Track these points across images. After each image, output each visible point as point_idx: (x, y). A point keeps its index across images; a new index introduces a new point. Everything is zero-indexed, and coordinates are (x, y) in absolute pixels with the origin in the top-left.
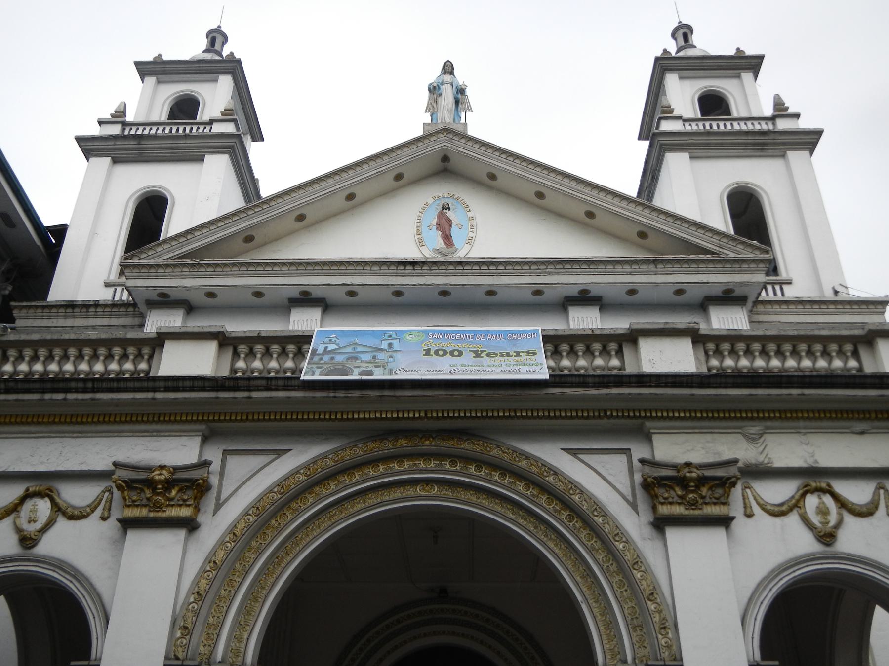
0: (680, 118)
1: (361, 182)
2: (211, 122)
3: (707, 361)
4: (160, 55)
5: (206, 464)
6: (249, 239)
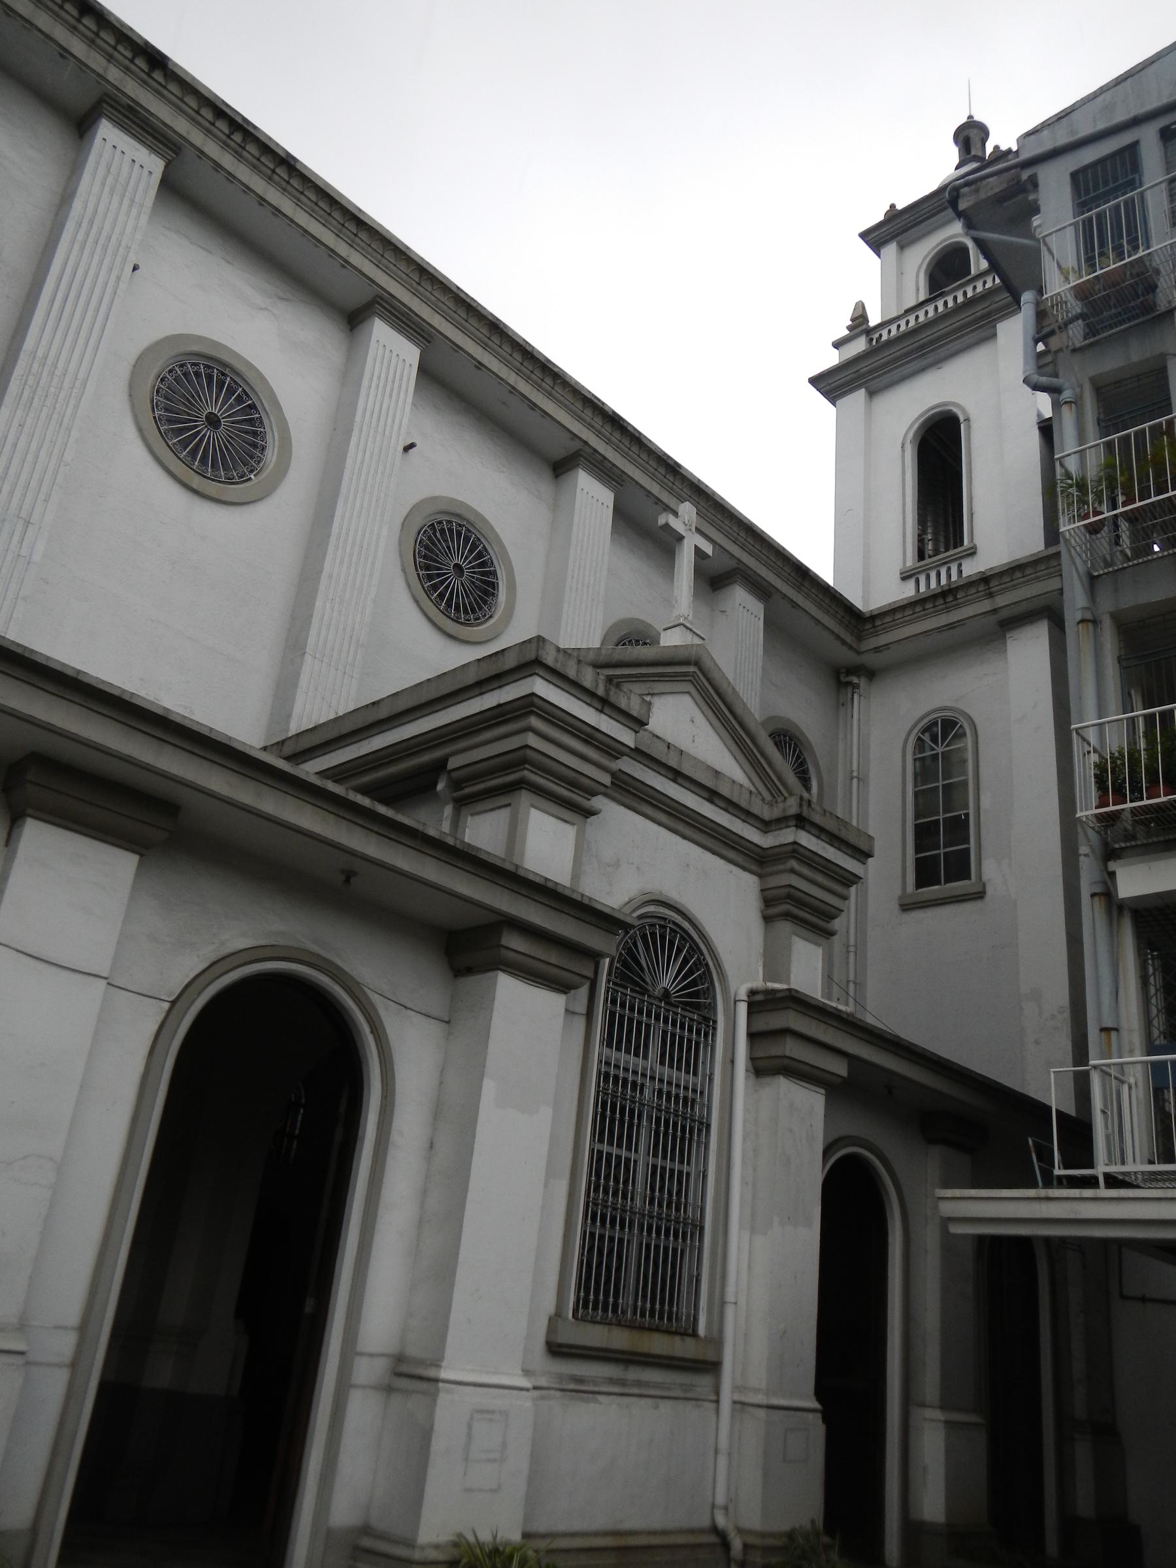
4: (893, 206)
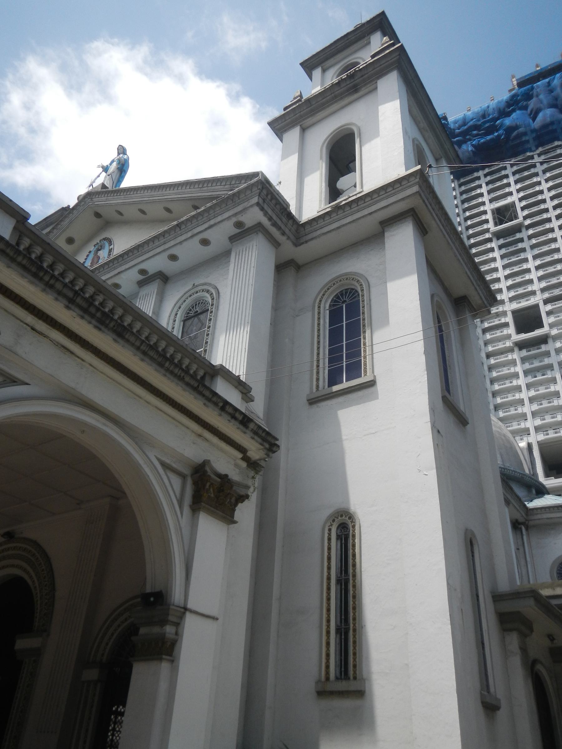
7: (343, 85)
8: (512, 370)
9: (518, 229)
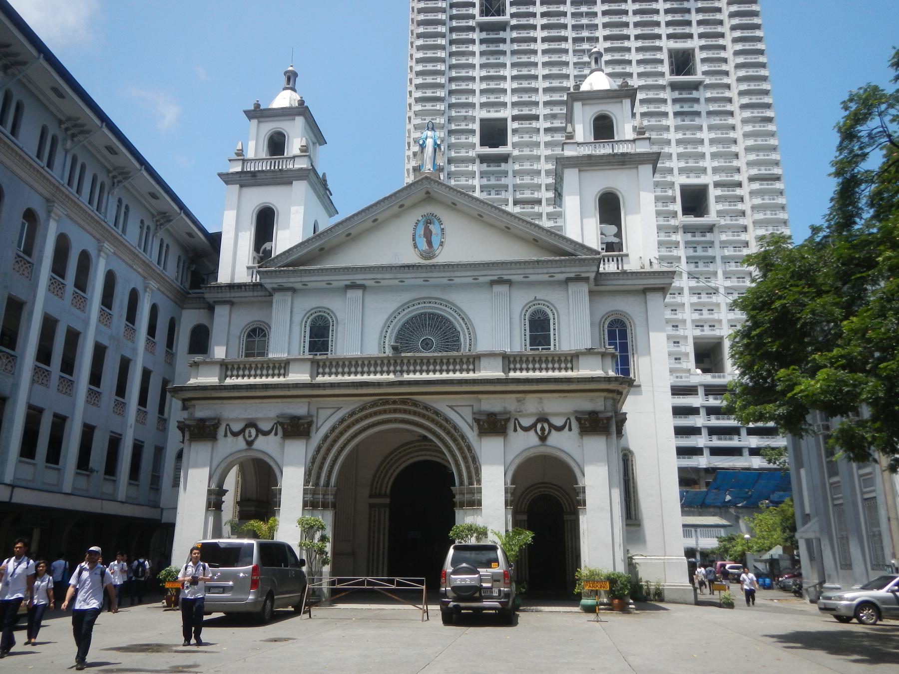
0: (576, 143)
1: (380, 213)
2: (294, 157)
3: (509, 365)
5: (310, 415)
6: (322, 249)
7: (616, 157)
8: (470, 182)
9: (503, 27)
